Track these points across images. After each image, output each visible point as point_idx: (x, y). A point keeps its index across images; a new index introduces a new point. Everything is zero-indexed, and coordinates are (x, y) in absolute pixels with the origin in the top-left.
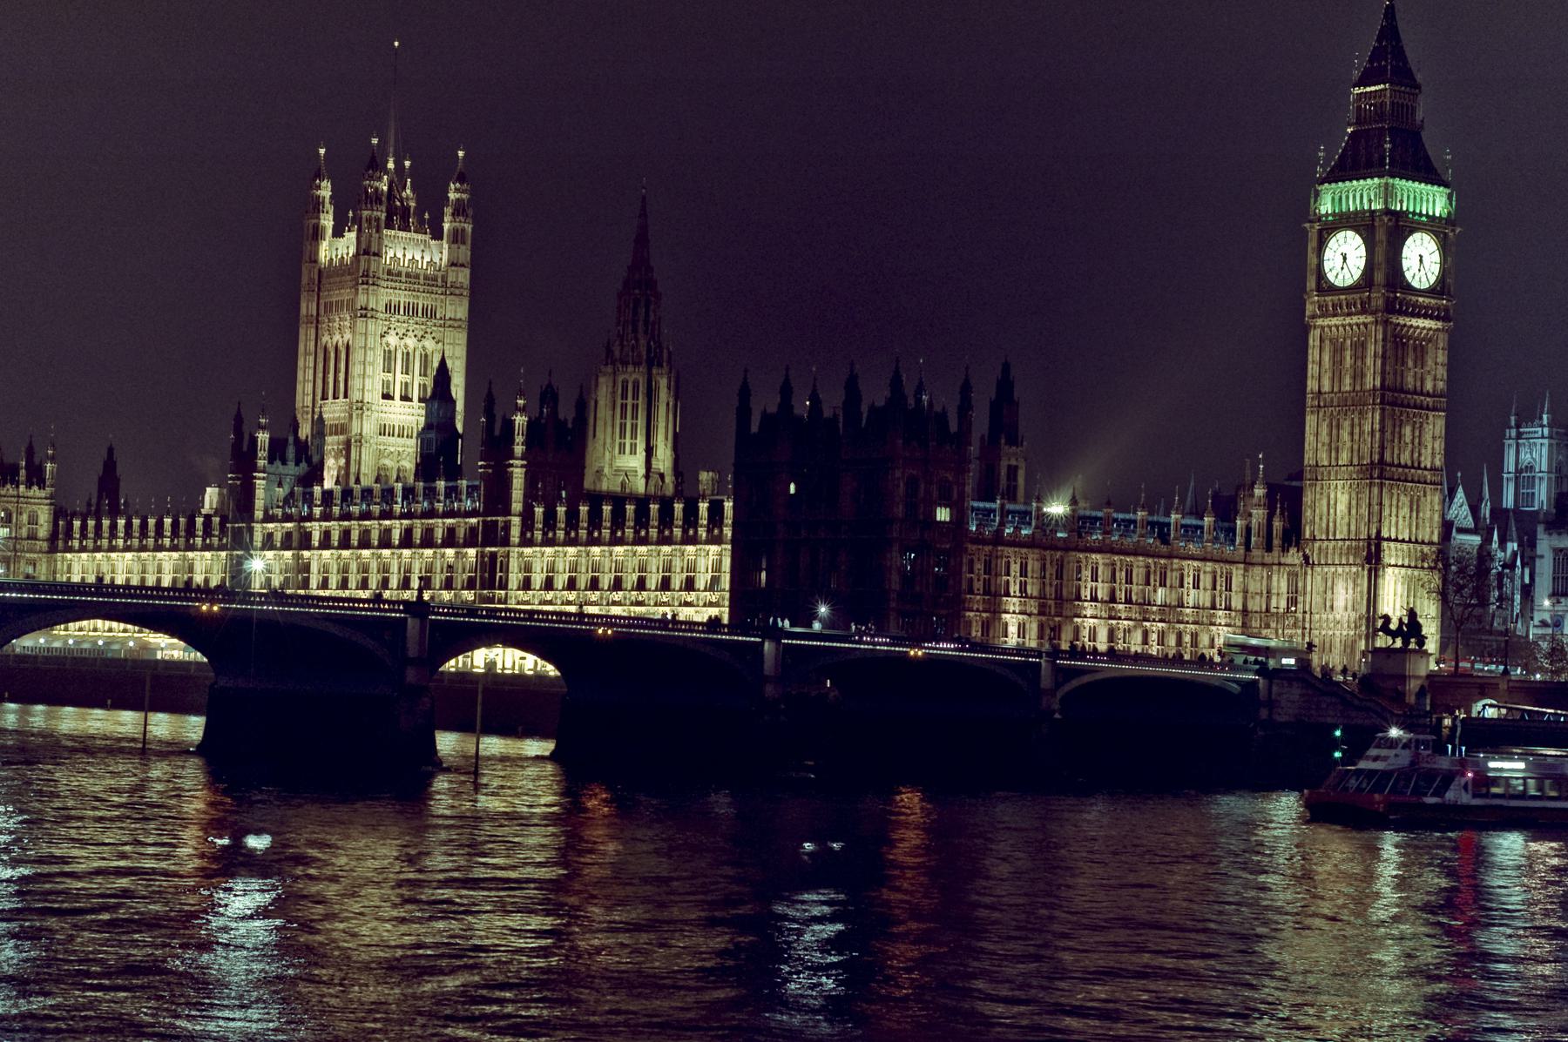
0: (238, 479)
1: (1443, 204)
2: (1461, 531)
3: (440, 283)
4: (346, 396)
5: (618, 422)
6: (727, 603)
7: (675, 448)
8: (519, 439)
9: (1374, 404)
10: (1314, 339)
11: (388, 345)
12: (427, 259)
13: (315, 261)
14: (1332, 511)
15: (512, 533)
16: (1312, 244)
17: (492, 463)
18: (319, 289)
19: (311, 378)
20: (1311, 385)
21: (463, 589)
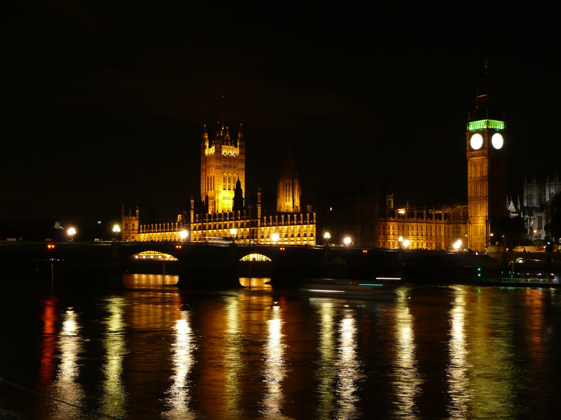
1: (503, 126)
2: (512, 213)
3: (237, 159)
4: (214, 190)
6: (315, 240)
7: (300, 200)
8: (259, 199)
11: (224, 176)
12: (234, 153)
14: (476, 209)
16: (468, 138)
18: (206, 162)
19: (204, 185)
20: (469, 176)
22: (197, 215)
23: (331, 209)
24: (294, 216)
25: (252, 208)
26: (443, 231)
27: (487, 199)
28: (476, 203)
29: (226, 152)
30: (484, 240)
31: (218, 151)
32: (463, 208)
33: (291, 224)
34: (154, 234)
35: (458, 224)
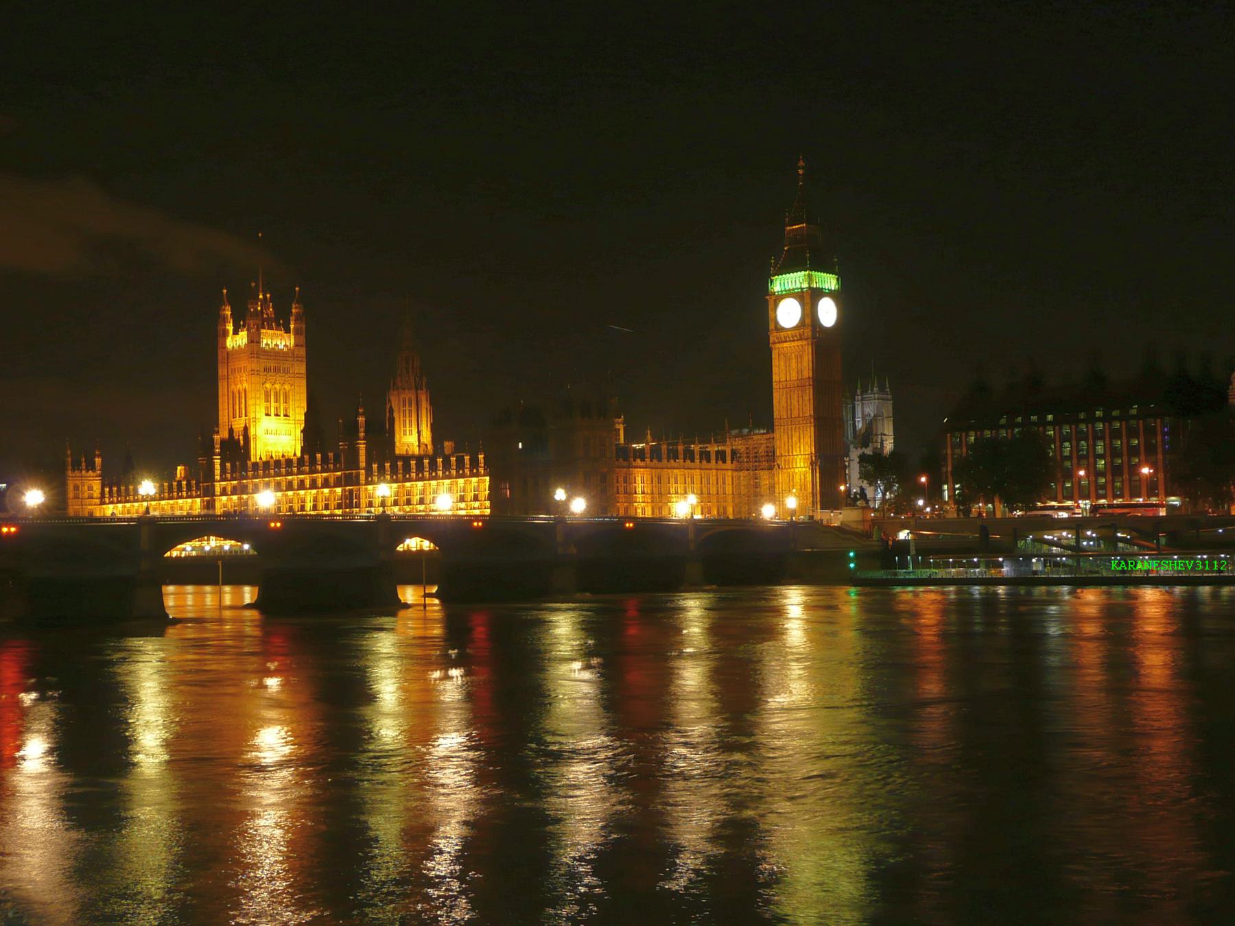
0: (346, 445)
1: (835, 283)
3: (291, 356)
4: (246, 416)
5: (402, 419)
7: (433, 431)
8: (362, 429)
9: (810, 385)
10: (775, 355)
11: (266, 388)
12: (283, 343)
13: (225, 347)
14: (790, 441)
15: (361, 478)
16: (771, 306)
17: (347, 443)
18: (228, 362)
20: (775, 378)
21: (335, 509)
22: (228, 465)
23: (520, 446)
24: (437, 461)
25: (346, 447)
26: (729, 485)
27: (812, 421)
28: (790, 429)
29: (269, 342)
30: (807, 499)
31: (254, 340)
32: (767, 439)
33: (431, 478)
34: (136, 504)
35: (755, 470)
